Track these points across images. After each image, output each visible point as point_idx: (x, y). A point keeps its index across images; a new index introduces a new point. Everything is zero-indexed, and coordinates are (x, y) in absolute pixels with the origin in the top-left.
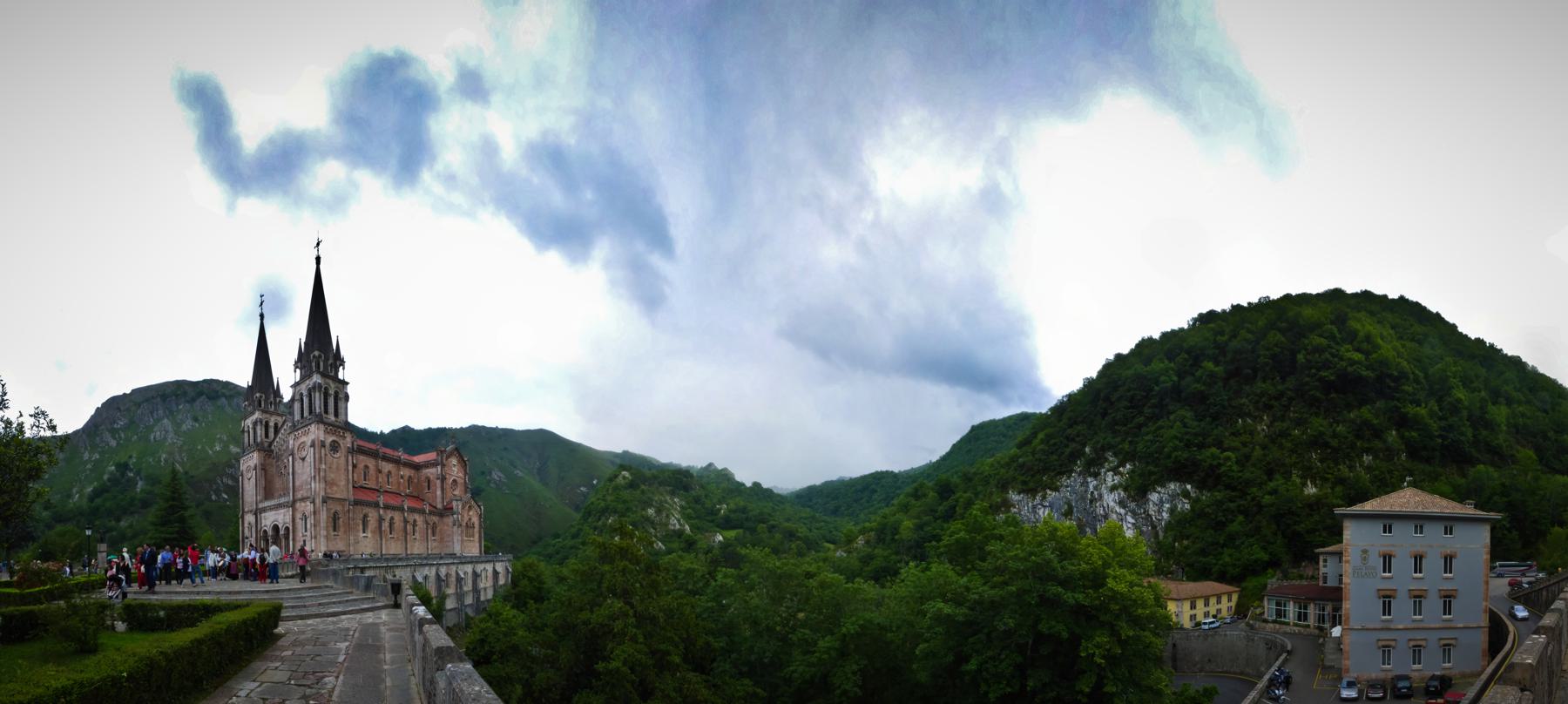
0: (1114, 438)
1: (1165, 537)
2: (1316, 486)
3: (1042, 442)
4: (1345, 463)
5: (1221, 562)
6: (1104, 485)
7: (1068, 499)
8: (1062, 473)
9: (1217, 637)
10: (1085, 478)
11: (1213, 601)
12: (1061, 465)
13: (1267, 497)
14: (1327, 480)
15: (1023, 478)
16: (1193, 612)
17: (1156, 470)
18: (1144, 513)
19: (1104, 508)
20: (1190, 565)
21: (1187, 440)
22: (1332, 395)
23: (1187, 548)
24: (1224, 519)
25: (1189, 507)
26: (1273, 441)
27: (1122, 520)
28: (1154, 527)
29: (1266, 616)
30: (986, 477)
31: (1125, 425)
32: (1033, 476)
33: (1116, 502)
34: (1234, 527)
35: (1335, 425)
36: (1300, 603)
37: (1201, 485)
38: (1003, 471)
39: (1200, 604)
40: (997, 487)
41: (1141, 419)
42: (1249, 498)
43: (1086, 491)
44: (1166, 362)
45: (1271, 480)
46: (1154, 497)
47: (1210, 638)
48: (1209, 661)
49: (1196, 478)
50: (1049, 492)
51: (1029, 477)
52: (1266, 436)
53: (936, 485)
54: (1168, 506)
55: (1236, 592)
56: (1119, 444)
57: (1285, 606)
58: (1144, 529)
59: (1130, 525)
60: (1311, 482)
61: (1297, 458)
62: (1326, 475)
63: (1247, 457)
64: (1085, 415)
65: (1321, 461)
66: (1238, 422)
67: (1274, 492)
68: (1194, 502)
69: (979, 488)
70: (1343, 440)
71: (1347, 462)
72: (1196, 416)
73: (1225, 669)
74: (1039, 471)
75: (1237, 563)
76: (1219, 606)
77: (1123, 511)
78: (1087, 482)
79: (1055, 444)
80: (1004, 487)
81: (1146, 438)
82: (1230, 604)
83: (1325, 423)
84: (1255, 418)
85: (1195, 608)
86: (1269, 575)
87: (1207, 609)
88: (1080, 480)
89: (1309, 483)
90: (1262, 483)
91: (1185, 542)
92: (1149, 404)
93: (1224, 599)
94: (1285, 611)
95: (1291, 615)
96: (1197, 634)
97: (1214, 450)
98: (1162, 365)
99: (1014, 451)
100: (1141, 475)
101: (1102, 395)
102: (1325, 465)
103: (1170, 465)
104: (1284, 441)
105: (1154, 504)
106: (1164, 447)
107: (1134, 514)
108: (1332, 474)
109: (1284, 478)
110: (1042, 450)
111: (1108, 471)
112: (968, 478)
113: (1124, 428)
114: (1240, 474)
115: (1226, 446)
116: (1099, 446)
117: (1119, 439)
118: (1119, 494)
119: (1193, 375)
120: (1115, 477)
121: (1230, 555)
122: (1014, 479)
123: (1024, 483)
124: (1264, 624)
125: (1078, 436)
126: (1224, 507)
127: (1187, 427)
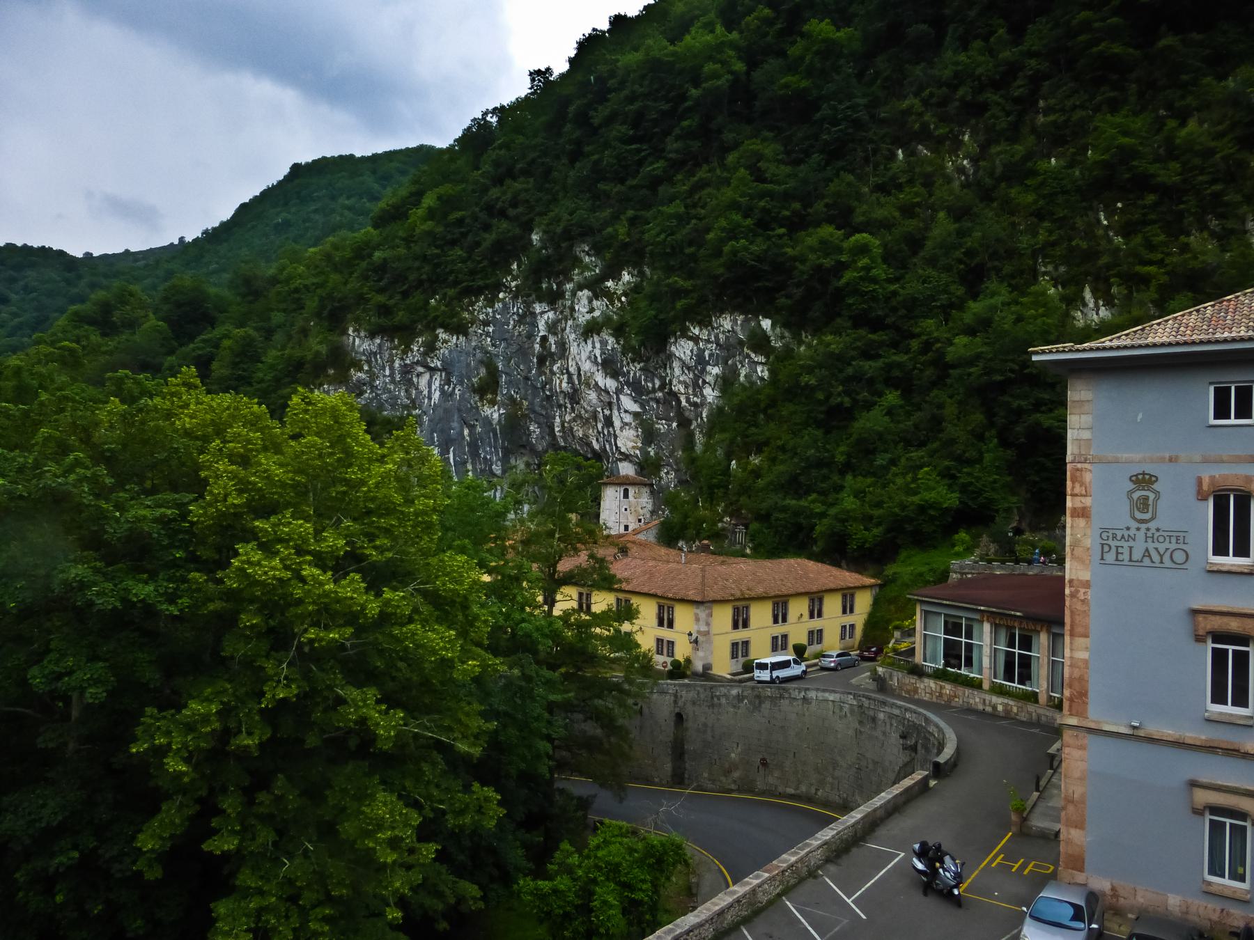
0: (593, 209)
1: (707, 447)
2: (1109, 303)
3: (431, 215)
4: (1203, 227)
5: (833, 511)
6: (570, 323)
7: (487, 352)
8: (478, 292)
9: (784, 703)
10: (528, 305)
11: (798, 608)
12: (472, 273)
13: (961, 340)
14: (1145, 280)
15: (381, 299)
16: (741, 635)
17: (688, 284)
18: (662, 388)
19: (570, 376)
20: (764, 517)
21: (764, 210)
22: (1163, 42)
23: (756, 473)
24: (847, 401)
25: (766, 375)
26: (987, 195)
27: (610, 404)
28: (684, 423)
29: (918, 658)
30: (297, 290)
31: (622, 181)
32: (405, 295)
33: (595, 362)
34: (872, 421)
35: (1172, 123)
36: (1010, 629)
37: (793, 321)
38: (335, 277)
39: (761, 614)
40: (318, 315)
41: (657, 167)
42: (915, 344)
43: (530, 336)
44: (719, 29)
45: (975, 297)
46: (683, 350)
47: (767, 705)
48: (764, 763)
49: (782, 301)
50: (442, 335)
51: (398, 297)
52: (966, 185)
53: (166, 299)
54: (716, 370)
55: (863, 587)
56: (606, 223)
57: (969, 635)
58: (662, 426)
59: (628, 418)
60: (1094, 292)
61: (1050, 232)
62: (1139, 268)
63: (915, 243)
64: (532, 155)
65: (1127, 231)
66: (893, 156)
67: (983, 325)
68: (778, 360)
69: (277, 318)
70: (1197, 161)
71: (1214, 223)
72: (787, 153)
73: (803, 788)
74: (420, 283)
75: (877, 512)
76: (816, 624)
77: (611, 384)
78: (533, 315)
79: (460, 222)
80: (335, 318)
81: (669, 210)
82: (848, 620)
83: (1138, 124)
84: (937, 144)
85: (746, 624)
86: (958, 549)
87: (779, 630)
88: (517, 308)
89: (1088, 295)
90: (951, 306)
91: (755, 460)
92: (677, 131)
93: (832, 605)
94: (969, 647)
95: (986, 662)
96: (734, 692)
97: (827, 231)
98: (709, 38)
99: (368, 231)
100: (653, 298)
101: (572, 109)
102: (1138, 240)
103: (721, 270)
104: (1013, 192)
105: (684, 365)
106: (708, 230)
107: (638, 391)
108: (1160, 263)
109: (1014, 288)
110: (429, 233)
111: (581, 288)
112: (250, 289)
113: (619, 188)
114: (893, 287)
115: (858, 219)
116: (559, 230)
117: (606, 213)
118: (604, 343)
119: (782, 54)
120: (596, 303)
121: (859, 494)
122: (361, 299)
123: (385, 310)
124: (912, 679)
125: (514, 204)
126: (850, 371)
127: (764, 181)
